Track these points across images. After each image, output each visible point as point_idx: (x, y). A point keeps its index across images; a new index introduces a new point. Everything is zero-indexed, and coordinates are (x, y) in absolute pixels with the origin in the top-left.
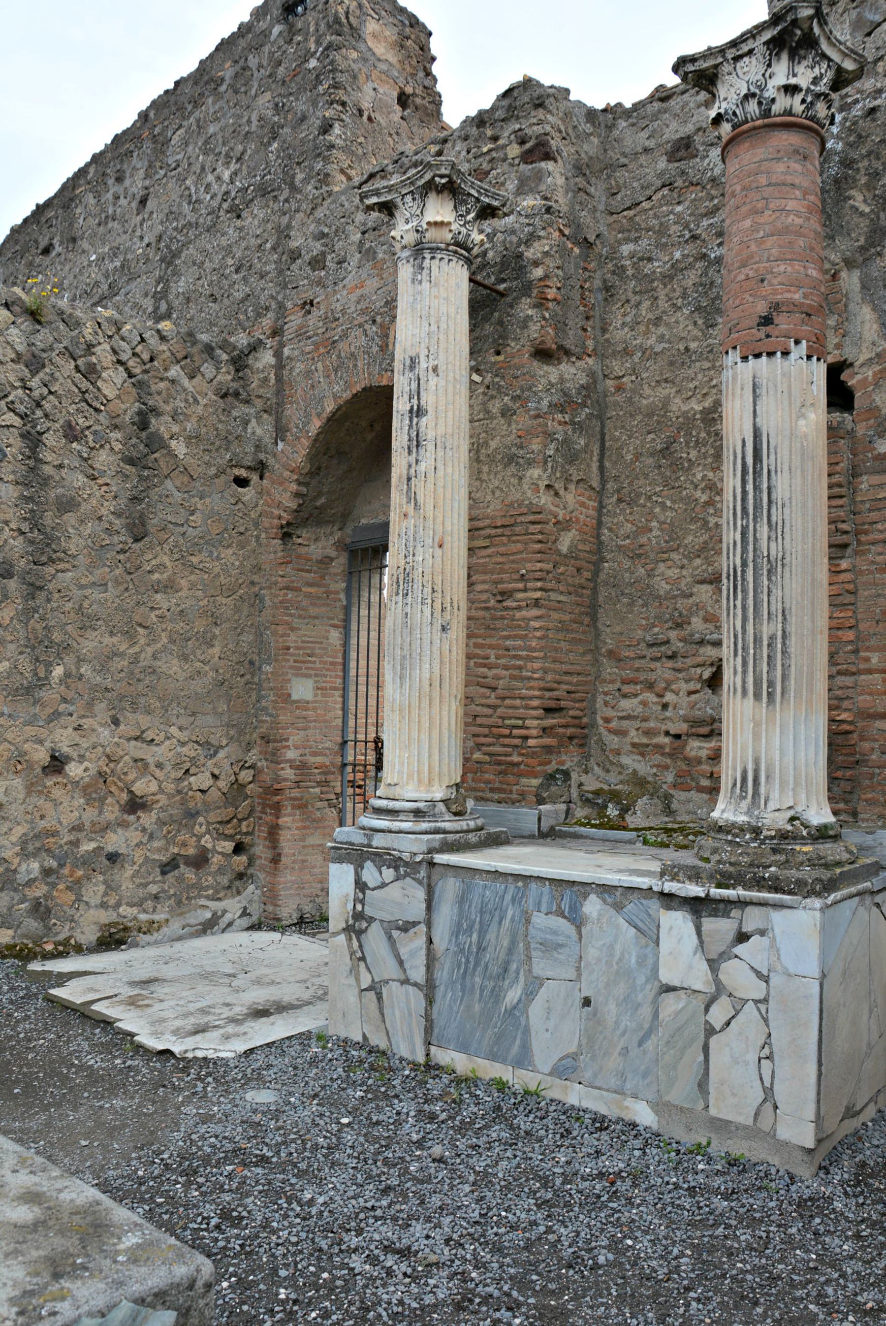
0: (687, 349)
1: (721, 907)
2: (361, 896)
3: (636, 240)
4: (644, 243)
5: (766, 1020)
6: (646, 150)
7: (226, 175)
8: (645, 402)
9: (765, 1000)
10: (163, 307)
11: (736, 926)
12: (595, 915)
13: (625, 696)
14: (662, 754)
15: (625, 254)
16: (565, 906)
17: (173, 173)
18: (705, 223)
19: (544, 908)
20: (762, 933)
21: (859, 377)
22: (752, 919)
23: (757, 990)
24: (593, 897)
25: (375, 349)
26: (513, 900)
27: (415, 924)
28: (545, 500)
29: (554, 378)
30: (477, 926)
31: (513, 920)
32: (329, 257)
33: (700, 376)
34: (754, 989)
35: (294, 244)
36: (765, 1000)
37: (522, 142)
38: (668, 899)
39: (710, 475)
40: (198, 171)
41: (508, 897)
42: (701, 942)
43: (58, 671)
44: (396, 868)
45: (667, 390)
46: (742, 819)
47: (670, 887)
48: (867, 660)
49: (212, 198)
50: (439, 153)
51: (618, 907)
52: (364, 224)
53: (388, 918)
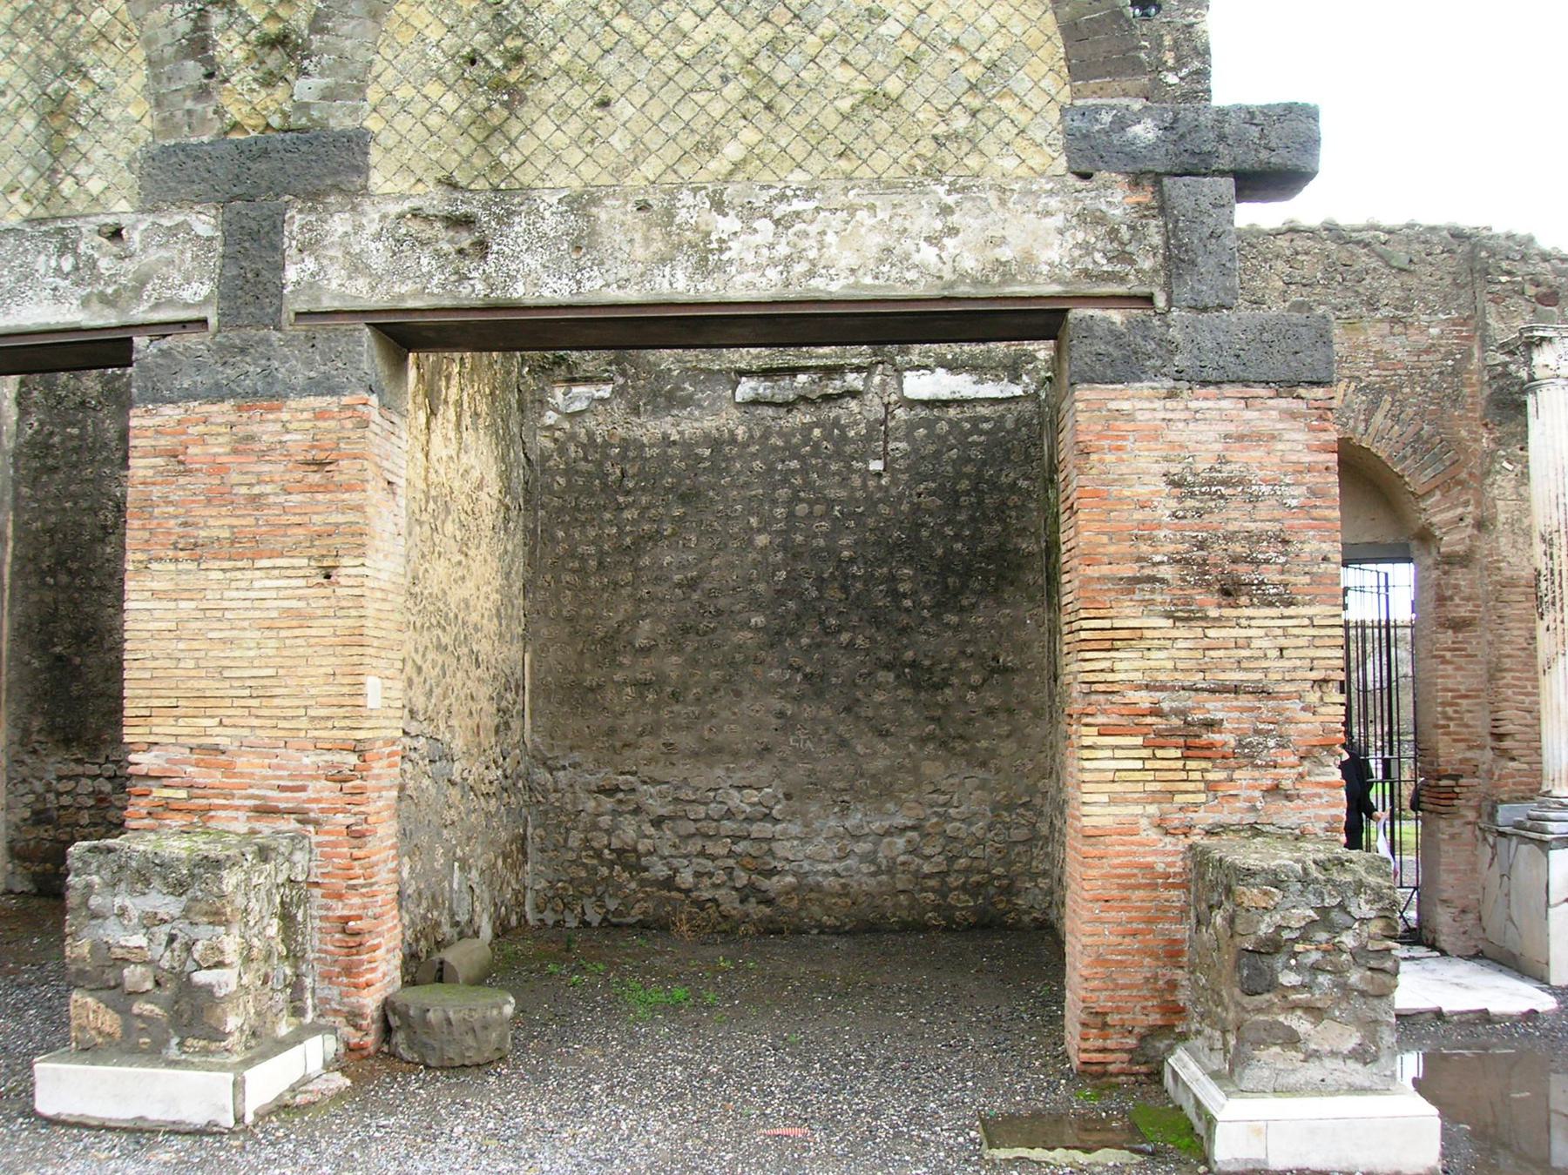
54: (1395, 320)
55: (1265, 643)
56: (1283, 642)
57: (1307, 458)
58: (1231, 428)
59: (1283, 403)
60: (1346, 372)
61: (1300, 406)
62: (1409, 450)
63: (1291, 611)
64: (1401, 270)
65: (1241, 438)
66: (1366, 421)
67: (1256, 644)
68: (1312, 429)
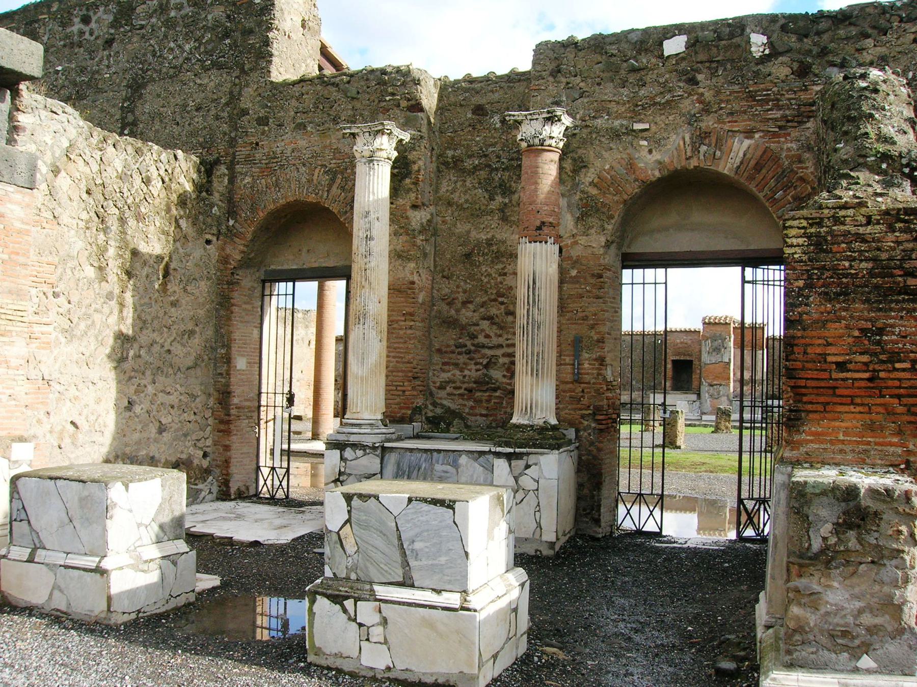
0: (480, 209)
1: (519, 456)
2: (344, 464)
3: (455, 150)
4: (459, 152)
5: (537, 497)
6: (461, 105)
7: (187, 47)
8: (457, 231)
9: (537, 490)
10: (130, 118)
11: (525, 462)
12: (464, 463)
13: (443, 371)
14: (463, 399)
15: (450, 155)
16: (451, 460)
17: (138, 32)
18: (491, 149)
19: (440, 462)
20: (536, 464)
21: (564, 243)
22: (532, 459)
23: (534, 486)
24: (464, 456)
25: (304, 180)
26: (425, 460)
27: (374, 475)
28: (416, 278)
29: (418, 218)
30: (407, 473)
31: (425, 468)
32: (271, 120)
33: (486, 223)
34: (532, 485)
35: (243, 106)
36: (537, 490)
38: (498, 455)
39: (489, 270)
40: (161, 37)
41: (423, 459)
42: (511, 470)
43: (131, 353)
44: (364, 450)
45: (468, 226)
46: (526, 422)
47: (499, 449)
48: (564, 360)
49: (174, 58)
50: (348, 82)
51: (476, 460)
52: (297, 108)
53: (360, 473)
60: (320, 163)
64: (353, 98)
66: (328, 191)
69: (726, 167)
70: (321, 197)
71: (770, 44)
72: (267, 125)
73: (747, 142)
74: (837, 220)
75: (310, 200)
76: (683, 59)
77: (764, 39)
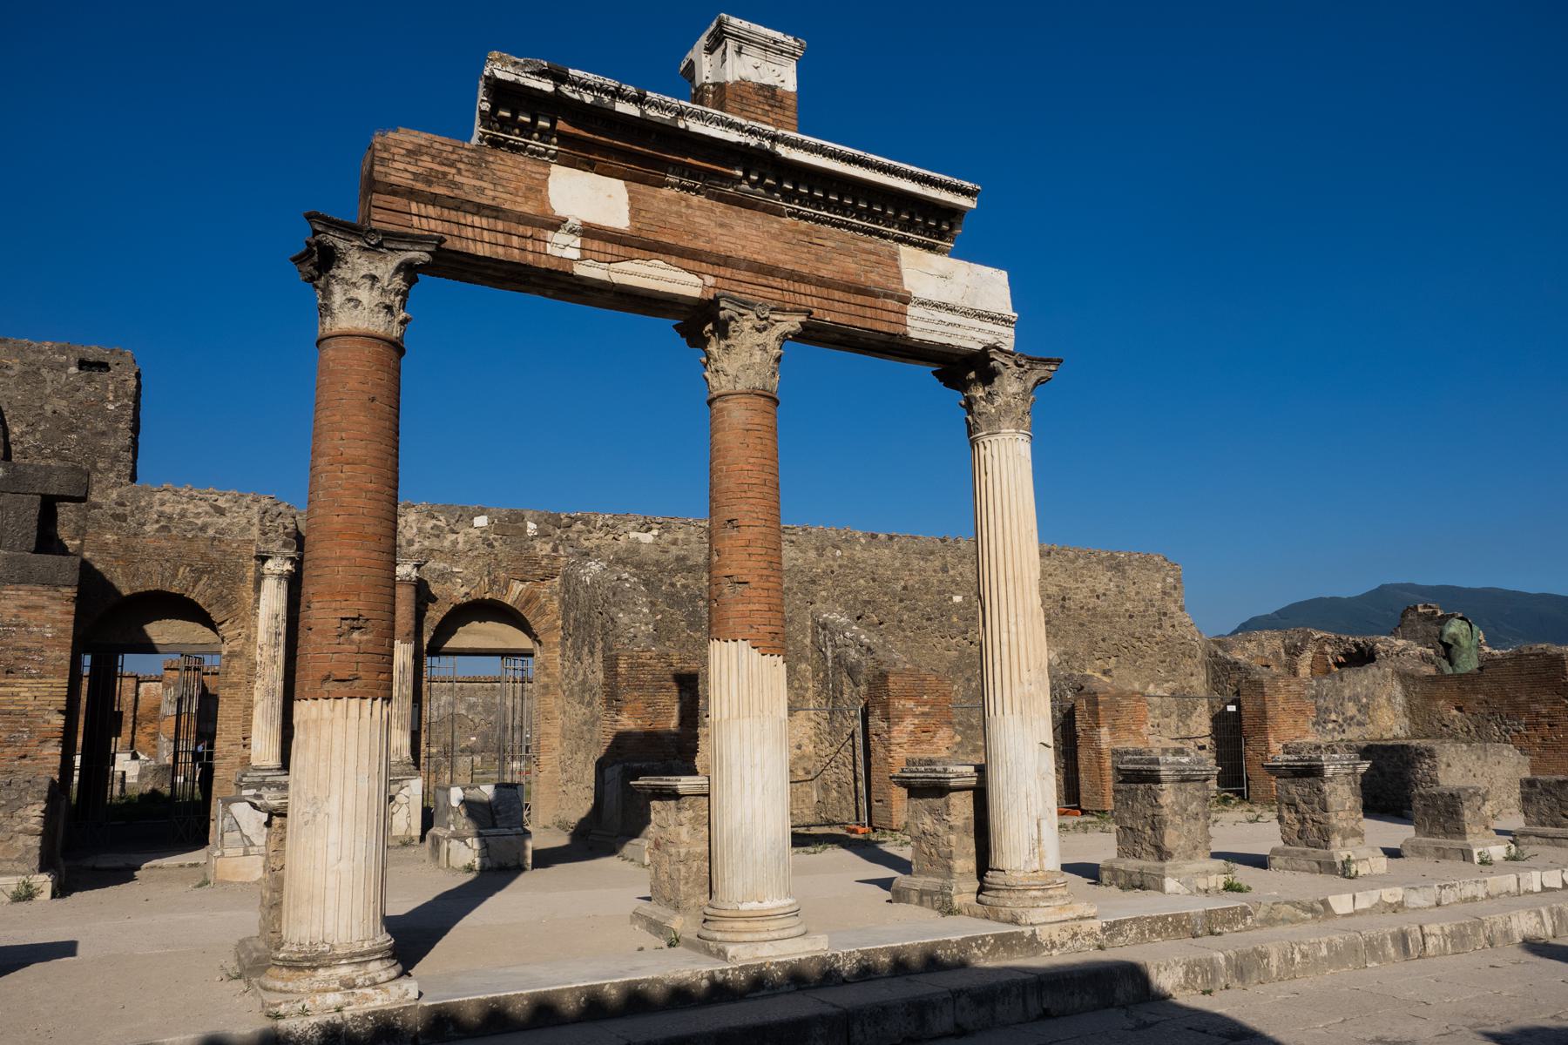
25: (167, 574)
37: (285, 528)
54: (214, 539)
55: (27, 694)
56: (37, 694)
57: (59, 617)
58: (23, 603)
59: (50, 593)
61: (57, 595)
62: (215, 601)
63: (43, 680)
65: (26, 607)
67: (22, 694)
68: (63, 604)
69: (509, 601)
70: (186, 590)
71: (538, 530)
72: (125, 521)
73: (522, 586)
74: (639, 658)
75: (173, 591)
76: (485, 531)
77: (535, 526)
